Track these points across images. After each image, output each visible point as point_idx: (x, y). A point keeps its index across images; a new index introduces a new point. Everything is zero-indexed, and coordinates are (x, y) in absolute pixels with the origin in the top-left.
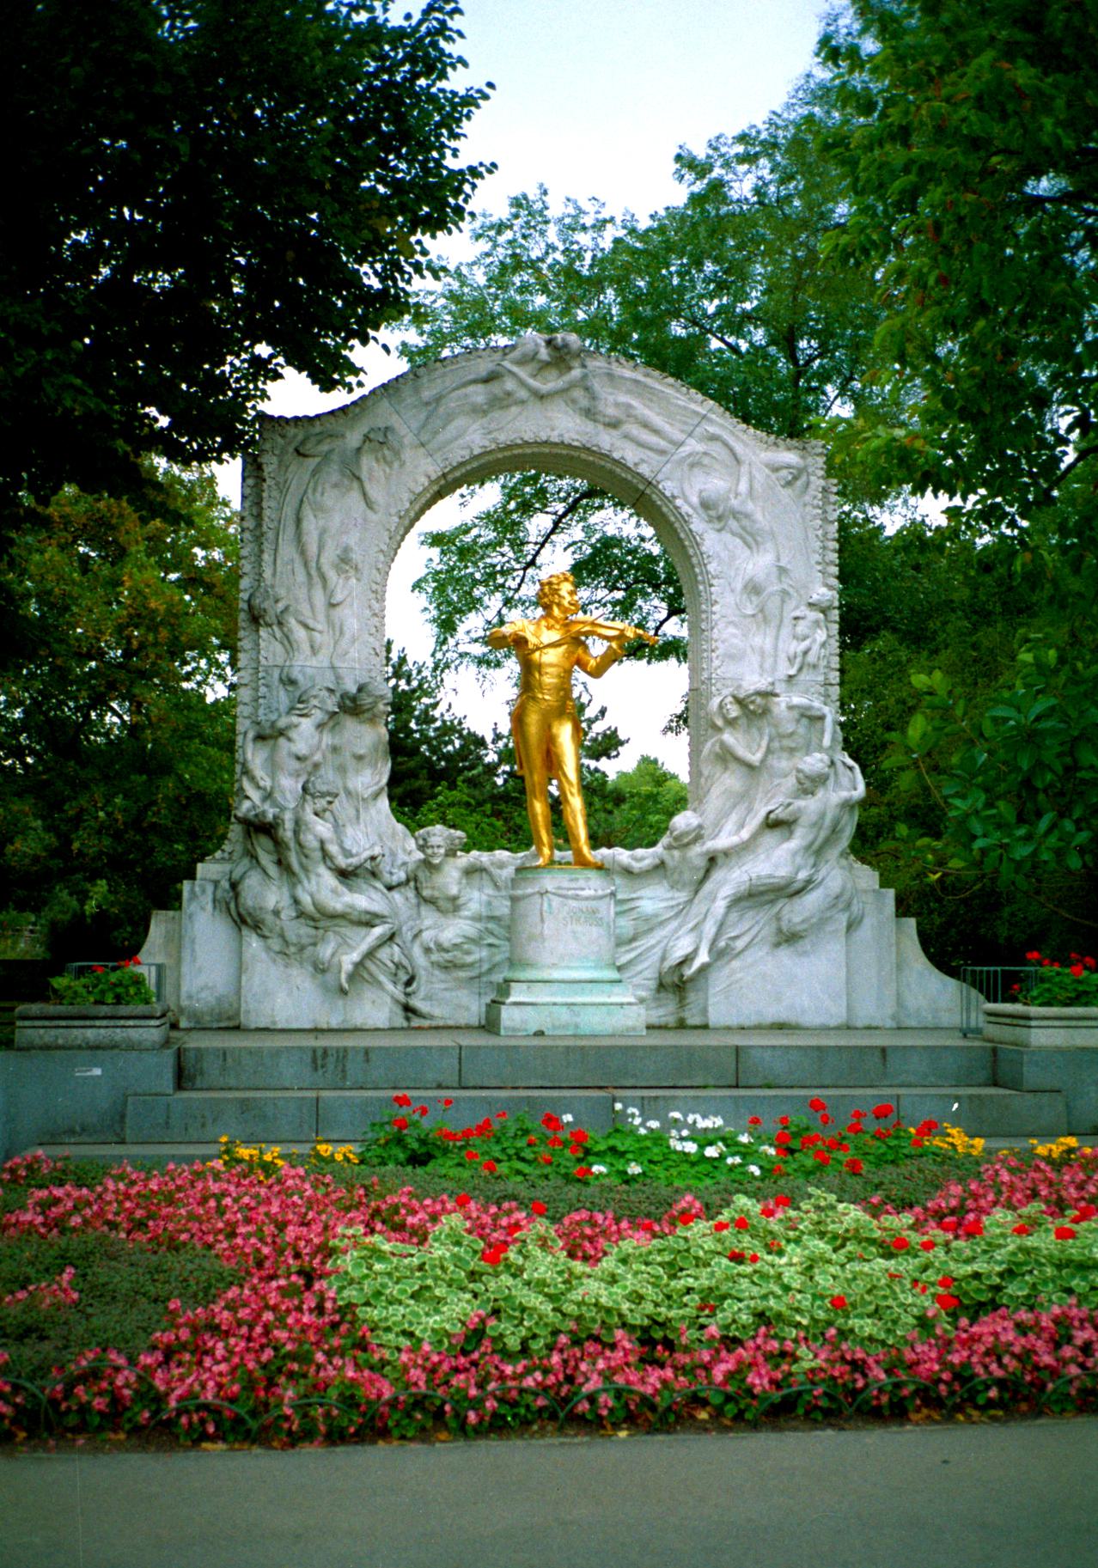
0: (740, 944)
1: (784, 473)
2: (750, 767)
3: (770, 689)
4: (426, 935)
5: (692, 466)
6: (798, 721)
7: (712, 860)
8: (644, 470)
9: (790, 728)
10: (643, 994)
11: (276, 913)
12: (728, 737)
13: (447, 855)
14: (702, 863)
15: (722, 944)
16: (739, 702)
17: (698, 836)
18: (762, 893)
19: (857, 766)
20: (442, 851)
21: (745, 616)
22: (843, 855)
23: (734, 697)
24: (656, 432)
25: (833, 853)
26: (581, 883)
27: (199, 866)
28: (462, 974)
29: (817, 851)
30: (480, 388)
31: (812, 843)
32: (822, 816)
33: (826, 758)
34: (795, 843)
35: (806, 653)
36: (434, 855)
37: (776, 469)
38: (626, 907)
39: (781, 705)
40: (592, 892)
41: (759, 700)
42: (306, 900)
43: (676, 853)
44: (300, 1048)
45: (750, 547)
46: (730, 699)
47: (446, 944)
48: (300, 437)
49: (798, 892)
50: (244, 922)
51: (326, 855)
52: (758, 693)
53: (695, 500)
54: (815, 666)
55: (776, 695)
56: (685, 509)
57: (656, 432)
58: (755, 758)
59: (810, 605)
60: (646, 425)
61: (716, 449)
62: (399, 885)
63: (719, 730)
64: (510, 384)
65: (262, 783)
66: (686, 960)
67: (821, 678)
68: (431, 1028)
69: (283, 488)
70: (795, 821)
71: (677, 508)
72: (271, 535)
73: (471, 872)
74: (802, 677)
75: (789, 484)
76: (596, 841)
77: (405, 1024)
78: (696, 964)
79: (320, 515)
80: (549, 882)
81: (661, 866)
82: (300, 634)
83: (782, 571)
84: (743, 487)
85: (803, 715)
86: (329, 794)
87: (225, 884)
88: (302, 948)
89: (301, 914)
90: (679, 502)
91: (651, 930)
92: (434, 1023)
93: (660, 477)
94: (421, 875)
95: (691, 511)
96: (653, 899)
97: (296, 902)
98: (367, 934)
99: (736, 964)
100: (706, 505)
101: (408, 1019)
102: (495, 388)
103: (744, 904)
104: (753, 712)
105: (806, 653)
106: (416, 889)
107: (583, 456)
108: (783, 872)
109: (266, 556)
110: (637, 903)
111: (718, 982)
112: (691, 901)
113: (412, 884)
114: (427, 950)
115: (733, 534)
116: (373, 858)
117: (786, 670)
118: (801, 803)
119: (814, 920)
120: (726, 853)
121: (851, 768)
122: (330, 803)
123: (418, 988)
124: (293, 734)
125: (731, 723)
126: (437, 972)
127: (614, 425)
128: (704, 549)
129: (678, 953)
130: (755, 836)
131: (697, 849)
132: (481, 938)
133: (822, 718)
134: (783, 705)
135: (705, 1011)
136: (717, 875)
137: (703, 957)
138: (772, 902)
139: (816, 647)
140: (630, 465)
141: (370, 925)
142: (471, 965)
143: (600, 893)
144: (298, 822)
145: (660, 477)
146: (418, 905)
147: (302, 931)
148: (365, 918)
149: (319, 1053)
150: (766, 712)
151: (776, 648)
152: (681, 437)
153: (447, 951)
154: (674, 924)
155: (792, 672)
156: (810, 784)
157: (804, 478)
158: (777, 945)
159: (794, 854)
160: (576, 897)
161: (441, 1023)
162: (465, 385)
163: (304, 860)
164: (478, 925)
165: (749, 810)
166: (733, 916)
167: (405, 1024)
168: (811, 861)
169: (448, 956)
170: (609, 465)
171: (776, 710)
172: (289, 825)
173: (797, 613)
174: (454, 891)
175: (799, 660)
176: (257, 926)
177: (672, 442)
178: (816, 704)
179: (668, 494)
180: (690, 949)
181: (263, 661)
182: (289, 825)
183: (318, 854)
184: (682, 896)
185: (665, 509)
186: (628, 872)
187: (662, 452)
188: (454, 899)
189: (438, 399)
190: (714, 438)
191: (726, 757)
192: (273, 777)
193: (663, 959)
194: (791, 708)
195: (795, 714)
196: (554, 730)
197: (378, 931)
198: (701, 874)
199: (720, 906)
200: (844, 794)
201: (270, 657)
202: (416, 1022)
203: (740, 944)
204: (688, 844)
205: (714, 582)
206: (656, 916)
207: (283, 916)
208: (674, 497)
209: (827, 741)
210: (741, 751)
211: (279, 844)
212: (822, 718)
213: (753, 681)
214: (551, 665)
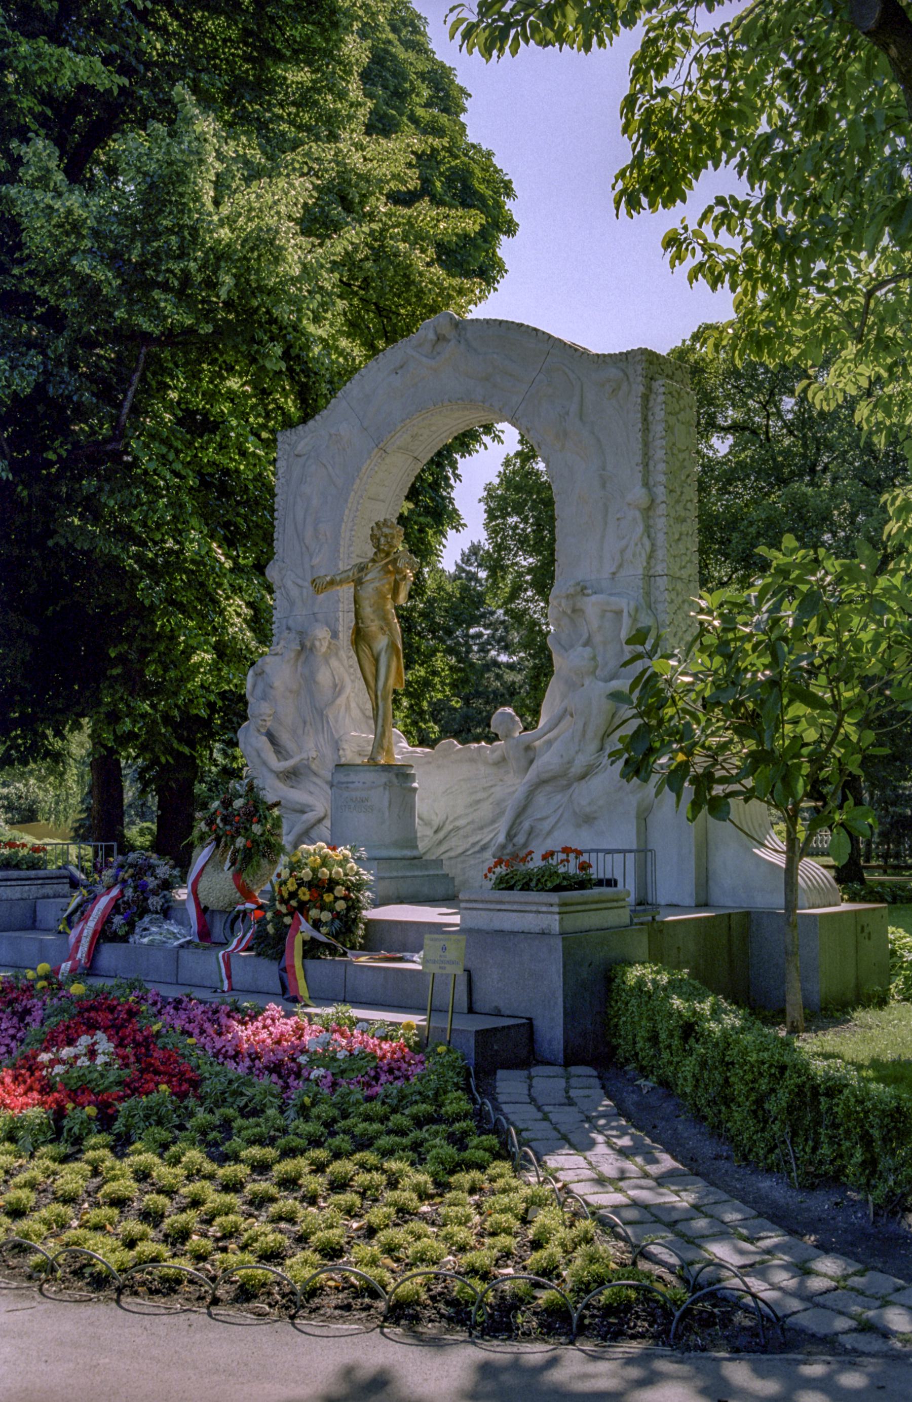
0: (547, 825)
6: (602, 617)
15: (526, 825)
35: (623, 551)
49: (583, 777)
103: (548, 788)
105: (623, 551)
138: (569, 785)
141: (303, 812)
148: (298, 807)
155: (613, 569)
157: (625, 387)
158: (578, 826)
166: (540, 798)
203: (547, 825)
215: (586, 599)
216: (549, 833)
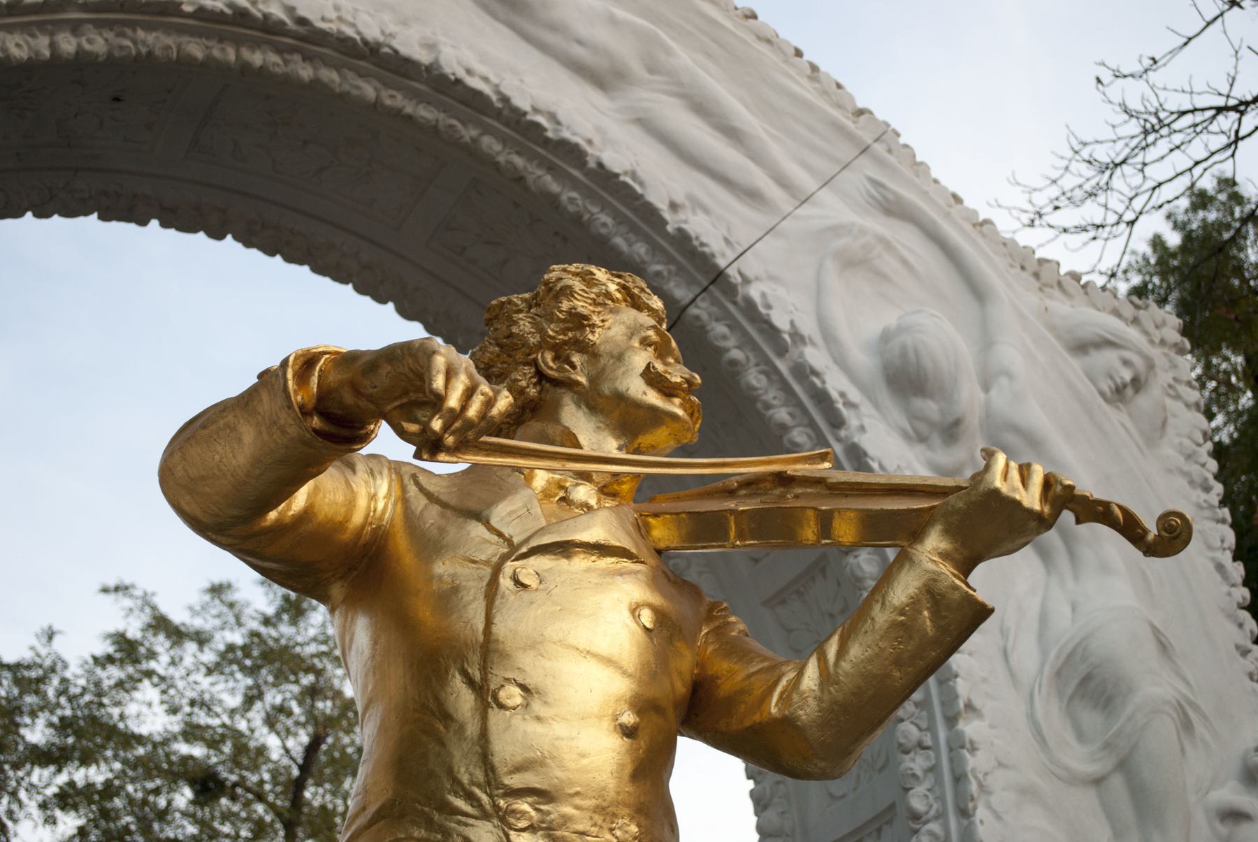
1: (1109, 358)
21: (1074, 780)
24: (732, 133)
53: (864, 361)
56: (835, 383)
57: (732, 133)
60: (702, 108)
71: (804, 372)
90: (815, 356)
95: (854, 395)
107: (490, 144)
127: (602, 77)
177: (783, 182)
179: (780, 320)
185: (754, 378)
208: (797, 337)
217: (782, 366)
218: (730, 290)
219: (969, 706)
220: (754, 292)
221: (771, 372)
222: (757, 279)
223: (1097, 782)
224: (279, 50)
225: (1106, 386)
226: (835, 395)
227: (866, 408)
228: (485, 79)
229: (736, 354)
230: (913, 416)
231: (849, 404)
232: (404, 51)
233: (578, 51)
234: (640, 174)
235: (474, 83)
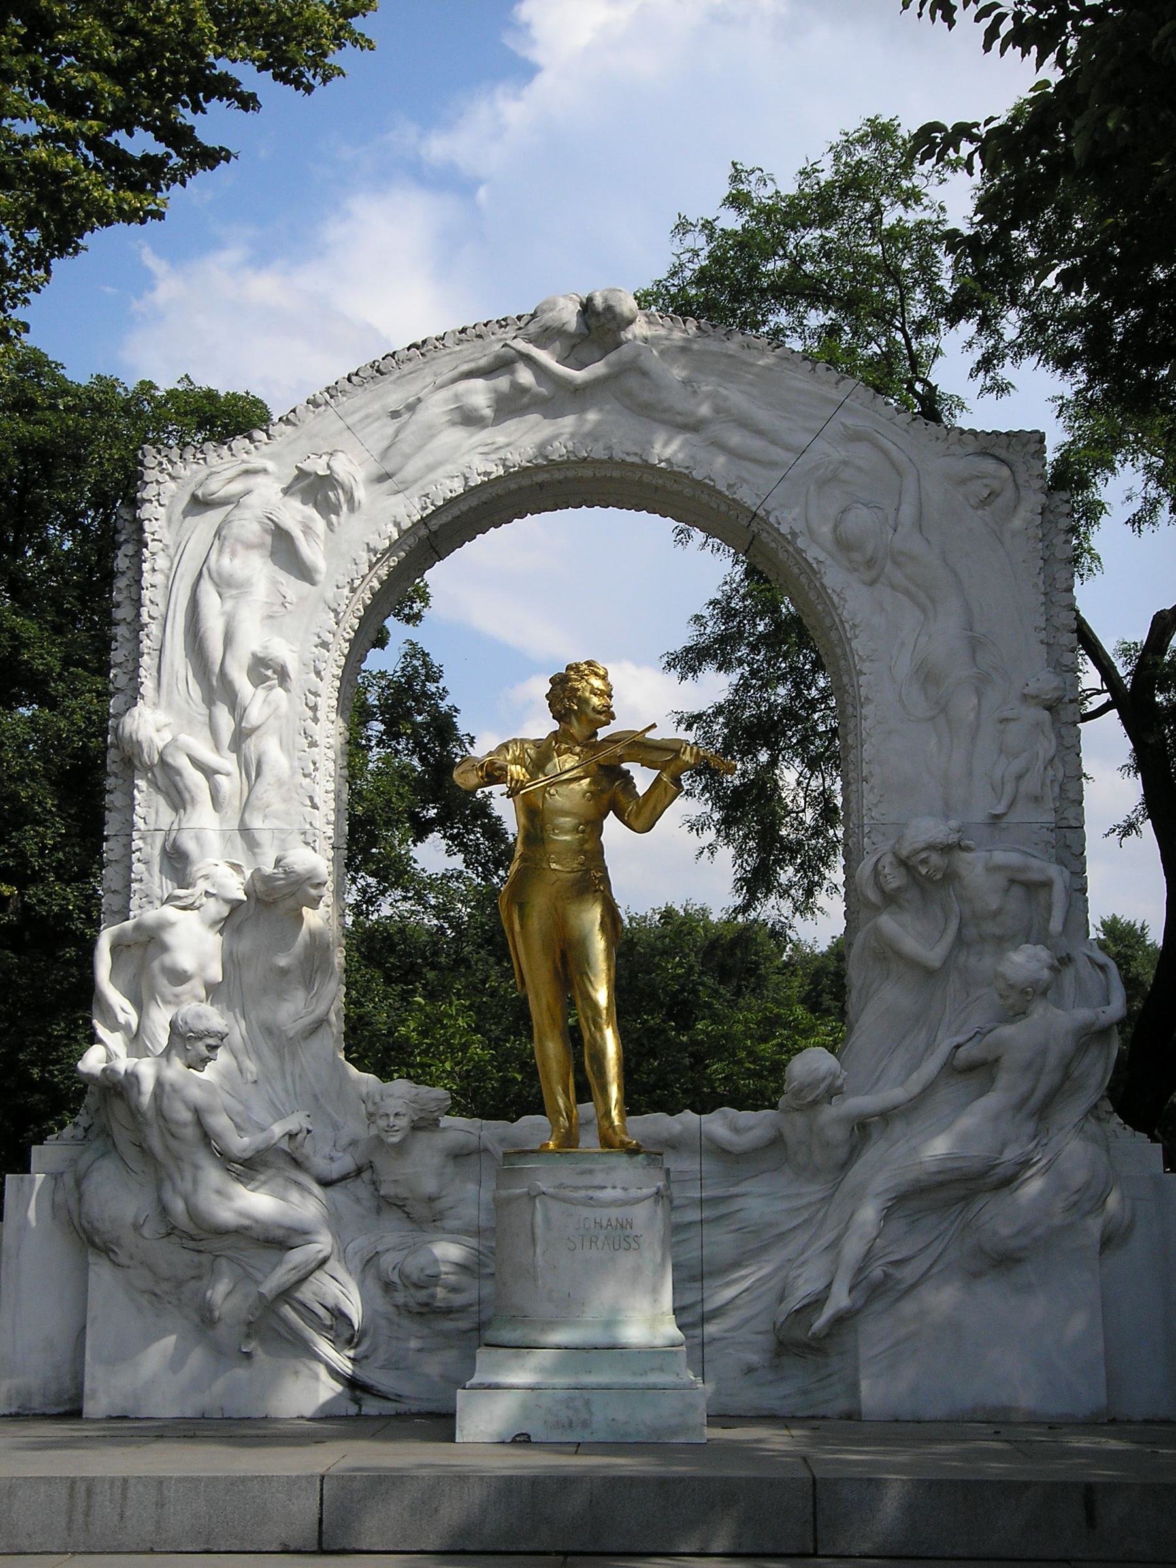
0: (908, 1274)
2: (929, 974)
3: (953, 838)
4: (388, 1261)
5: (823, 483)
7: (862, 1129)
8: (747, 496)
9: (994, 903)
10: (754, 1358)
11: (137, 1227)
12: (887, 922)
13: (416, 1127)
14: (838, 1134)
15: (877, 1272)
16: (903, 863)
17: (833, 1092)
18: (941, 1185)
19: (1112, 965)
20: (403, 1122)
22: (1093, 1111)
23: (895, 855)
25: (1072, 1112)
26: (599, 1179)
27: (35, 1149)
28: (448, 1325)
29: (1041, 1111)
30: (479, 383)
31: (1024, 1101)
32: (1043, 1052)
33: (1043, 953)
34: (992, 1101)
36: (390, 1129)
37: (963, 482)
38: (723, 1209)
39: (974, 867)
40: (618, 1193)
41: (935, 859)
42: (179, 1206)
43: (799, 1120)
44: (49, 1480)
45: (924, 610)
46: (888, 859)
47: (415, 1277)
48: (202, 475)
50: (93, 1244)
51: (206, 1137)
52: (930, 847)
54: (1037, 799)
55: (968, 849)
56: (813, 553)
57: (760, 433)
58: (933, 956)
59: (1025, 697)
60: (744, 424)
61: (862, 453)
62: (343, 1178)
63: (877, 910)
64: (525, 376)
65: (122, 1018)
66: (818, 1302)
67: (1049, 818)
68: (398, 1415)
69: (176, 556)
70: (997, 1060)
71: (800, 551)
72: (154, 628)
73: (459, 1155)
74: (1013, 818)
75: (984, 502)
76: (631, 1106)
77: (353, 1410)
78: (828, 1312)
79: (229, 593)
80: (545, 1177)
81: (777, 1142)
82: (195, 779)
83: (975, 645)
84: (908, 512)
85: (1012, 881)
86: (209, 1034)
87: (69, 1180)
88: (180, 1284)
89: (171, 1231)
90: (801, 543)
91: (764, 1248)
92: (402, 1407)
93: (771, 504)
94: (378, 1161)
95: (822, 556)
96: (761, 1200)
97: (164, 1210)
98: (280, 1262)
99: (908, 1307)
100: (844, 545)
101: (357, 1401)
102: (502, 383)
104: (928, 878)
105: (1019, 777)
106: (374, 1183)
107: (647, 478)
108: (978, 1151)
109: (145, 661)
110: (737, 1204)
111: (875, 1335)
112: (827, 1199)
113: (366, 1176)
114: (388, 1287)
115: (893, 587)
116: (292, 1136)
117: (983, 805)
118: (1007, 1031)
119: (1038, 1231)
120: (886, 1116)
121: (1102, 968)
122: (212, 1048)
123: (374, 1349)
124: (170, 938)
125: (890, 899)
126: (405, 1322)
127: (693, 426)
128: (846, 615)
129: (804, 1288)
130: (929, 1089)
131: (830, 1112)
132: (480, 1264)
133: (1047, 884)
134: (980, 868)
135: (855, 1387)
136: (871, 1154)
137: (840, 1299)
138: (967, 1199)
139: (1040, 764)
140: (721, 487)
142: (463, 1309)
143: (634, 1193)
144: (159, 1083)
145: (771, 504)
146: (379, 1211)
147: (174, 1258)
148: (279, 1233)
149: (81, 1488)
150: (950, 877)
151: (970, 774)
152: (804, 439)
153: (419, 1286)
154: (802, 1238)
155: (1000, 810)
156: (1020, 1000)
158: (976, 1275)
159: (996, 1118)
160: (590, 1202)
161: (414, 1407)
162: (454, 381)
163: (172, 1143)
164: (473, 1242)
165: (930, 1045)
167: (353, 1410)
168: (1030, 1127)
169: (422, 1295)
170: (688, 492)
171: (963, 872)
172: (148, 1086)
173: (1008, 714)
174: (429, 1186)
175: (1009, 789)
176: (106, 1250)
178: (1035, 863)
179: (784, 529)
180: (820, 1285)
181: (140, 823)
182: (148, 1086)
183: (190, 1132)
184: (814, 1191)
185: (782, 555)
186: (720, 1152)
187: (771, 465)
188: (431, 1199)
189: (411, 408)
190: (856, 437)
191: (887, 955)
192: (139, 1006)
193: (782, 1298)
194: (992, 869)
195: (1001, 880)
196: (572, 921)
197: (296, 1257)
198: (842, 1153)
199: (869, 1214)
200: (1083, 1014)
201: (151, 819)
202: (372, 1407)
203: (908, 1274)
204: (815, 1103)
205: (866, 667)
206: (771, 1225)
207: (146, 1232)
208: (794, 534)
209: (1056, 925)
210: (910, 944)
211: (134, 1112)
212: (1047, 884)
213: (928, 829)
214: (565, 813)
215: (965, 855)
216: (913, 1286)
217: (791, 549)
218: (762, 519)
219: (867, 698)
220: (772, 519)
221: (787, 551)
222: (774, 509)
223: (932, 718)
224: (547, 472)
225: (972, 502)
226: (811, 560)
227: (829, 562)
228: (636, 454)
229: (773, 545)
230: (851, 562)
231: (819, 562)
232: (596, 457)
233: (679, 419)
234: (713, 477)
235: (629, 459)
